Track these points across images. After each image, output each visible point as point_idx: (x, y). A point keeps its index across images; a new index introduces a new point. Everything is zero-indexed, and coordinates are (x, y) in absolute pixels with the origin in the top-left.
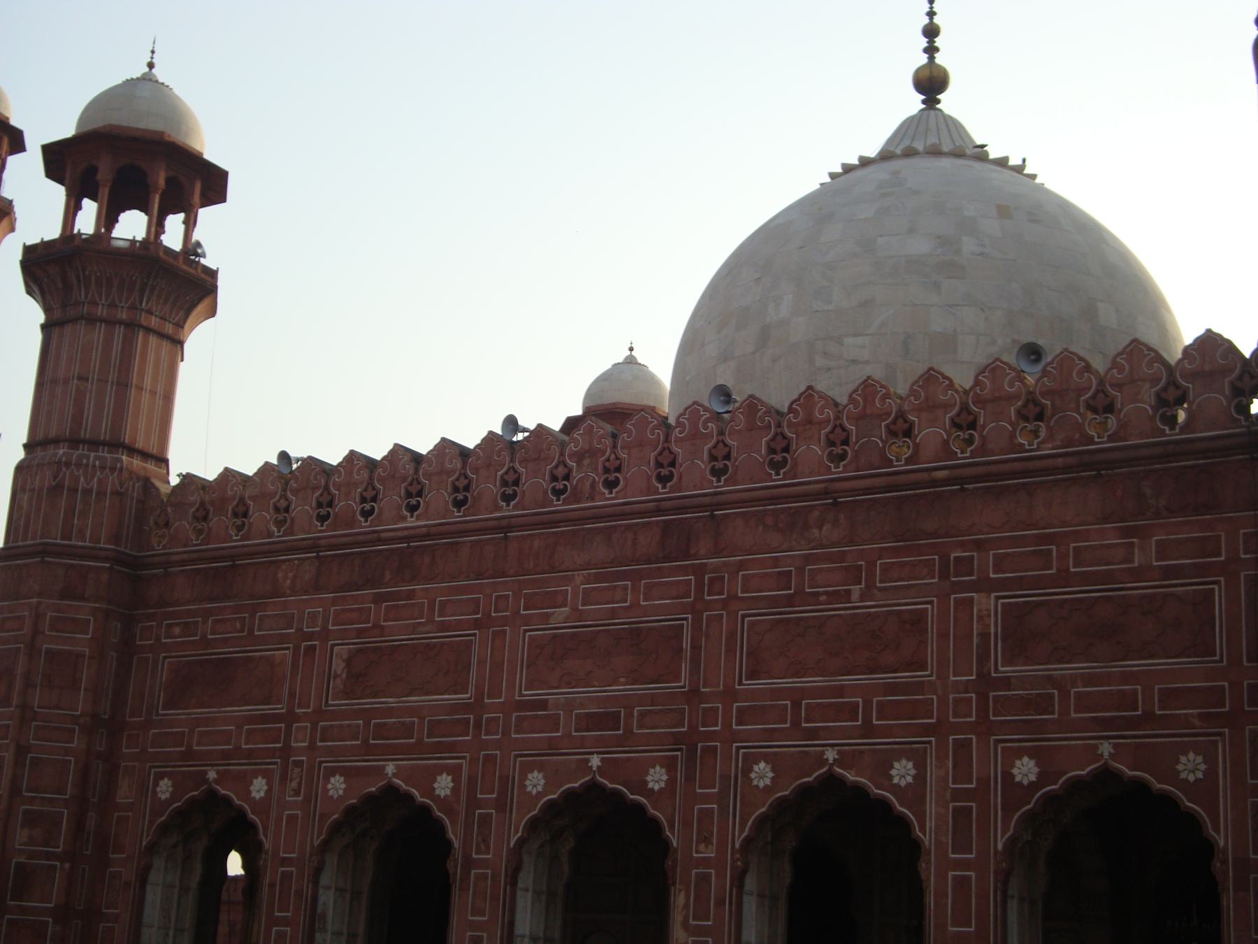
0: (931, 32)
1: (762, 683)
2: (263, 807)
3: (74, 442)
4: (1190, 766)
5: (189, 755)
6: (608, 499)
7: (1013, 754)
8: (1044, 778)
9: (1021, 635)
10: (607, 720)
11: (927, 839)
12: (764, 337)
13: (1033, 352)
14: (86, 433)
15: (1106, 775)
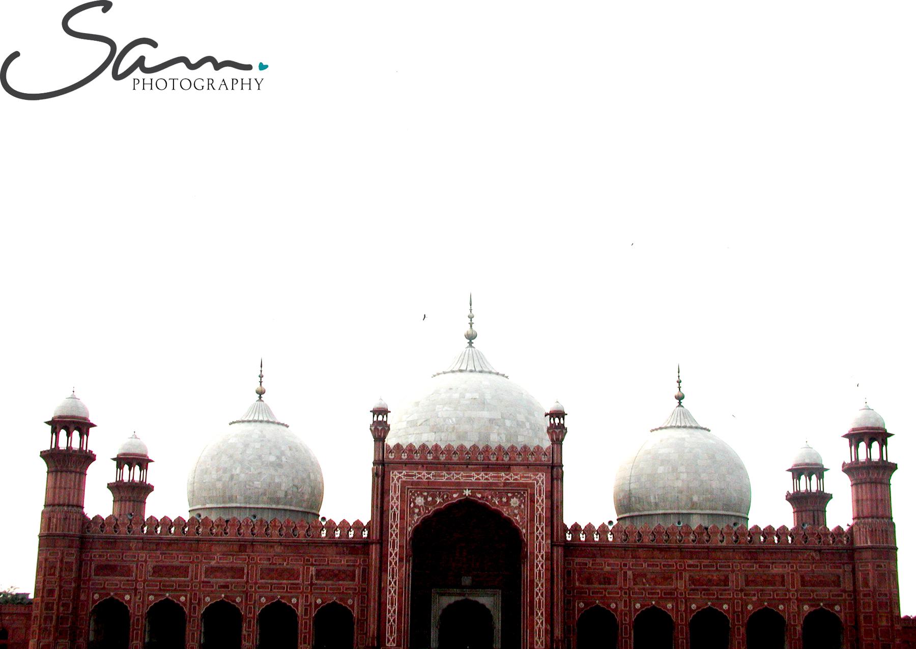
0: (261, 377)
1: (263, 581)
2: (129, 601)
3: (68, 506)
4: (350, 602)
5: (104, 588)
6: (225, 537)
7: (316, 598)
8: (323, 603)
9: (319, 574)
10: (226, 586)
11: (299, 613)
12: (232, 477)
13: (324, 519)
14: (71, 503)
15: (334, 603)
